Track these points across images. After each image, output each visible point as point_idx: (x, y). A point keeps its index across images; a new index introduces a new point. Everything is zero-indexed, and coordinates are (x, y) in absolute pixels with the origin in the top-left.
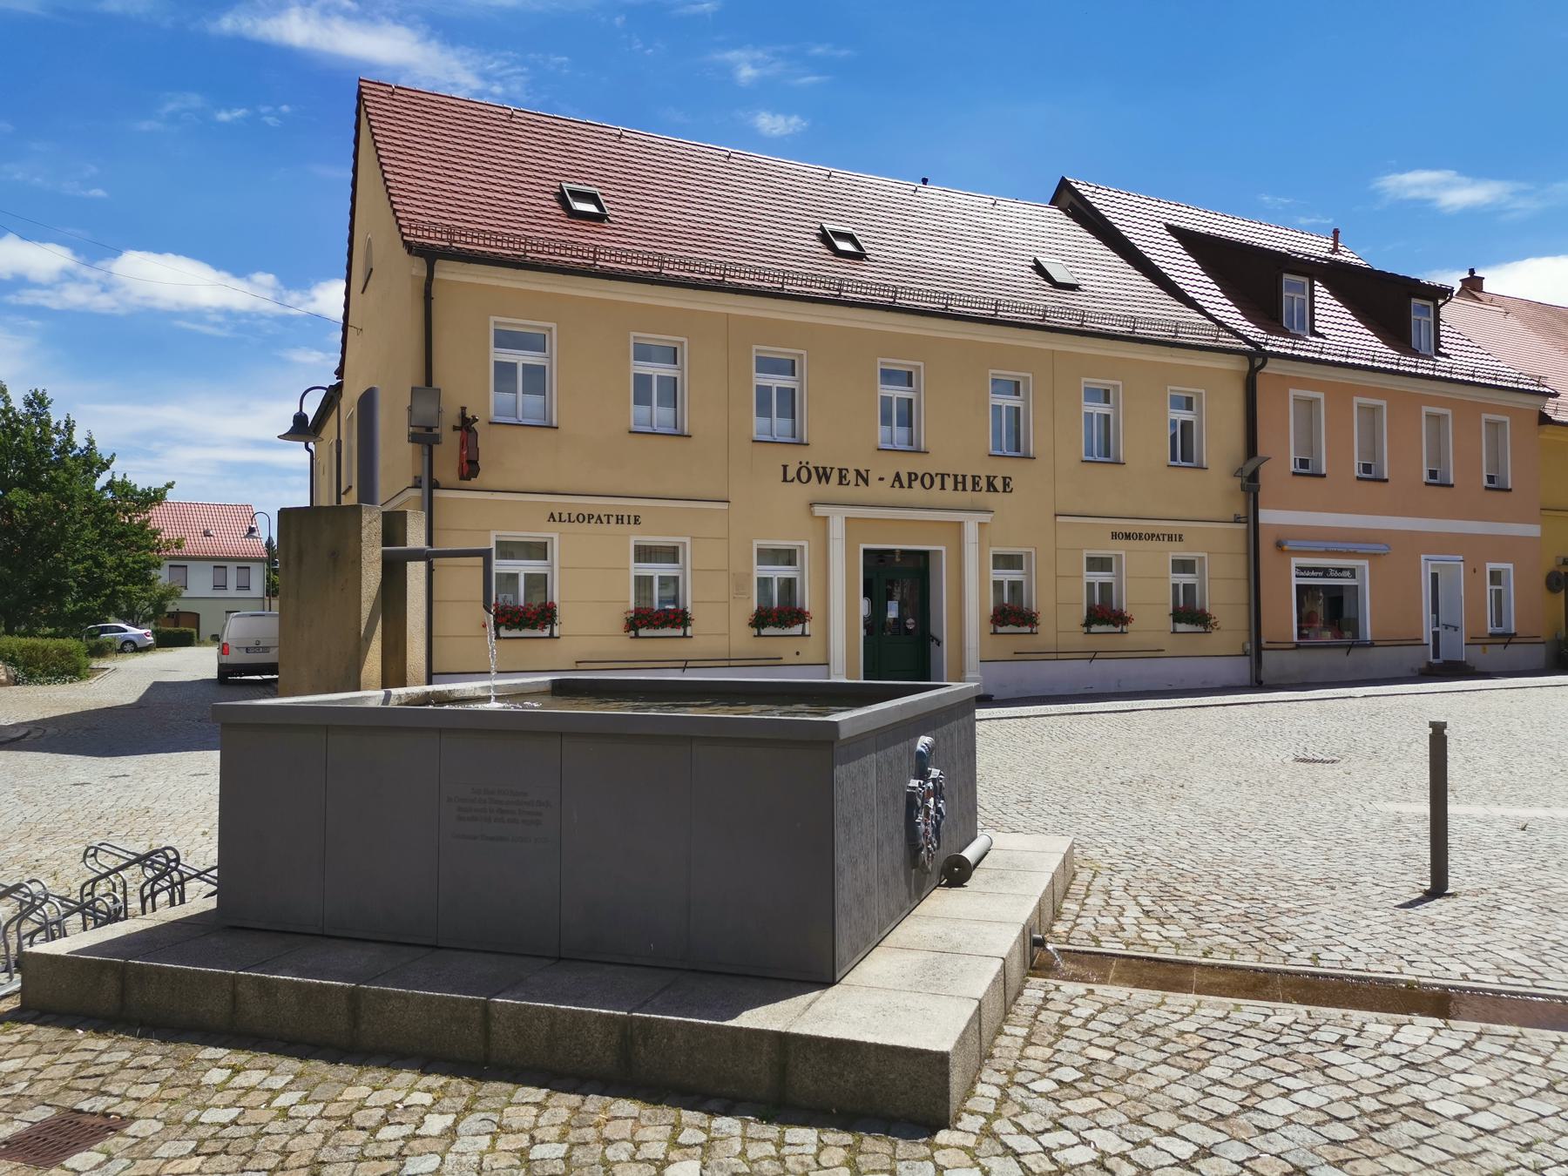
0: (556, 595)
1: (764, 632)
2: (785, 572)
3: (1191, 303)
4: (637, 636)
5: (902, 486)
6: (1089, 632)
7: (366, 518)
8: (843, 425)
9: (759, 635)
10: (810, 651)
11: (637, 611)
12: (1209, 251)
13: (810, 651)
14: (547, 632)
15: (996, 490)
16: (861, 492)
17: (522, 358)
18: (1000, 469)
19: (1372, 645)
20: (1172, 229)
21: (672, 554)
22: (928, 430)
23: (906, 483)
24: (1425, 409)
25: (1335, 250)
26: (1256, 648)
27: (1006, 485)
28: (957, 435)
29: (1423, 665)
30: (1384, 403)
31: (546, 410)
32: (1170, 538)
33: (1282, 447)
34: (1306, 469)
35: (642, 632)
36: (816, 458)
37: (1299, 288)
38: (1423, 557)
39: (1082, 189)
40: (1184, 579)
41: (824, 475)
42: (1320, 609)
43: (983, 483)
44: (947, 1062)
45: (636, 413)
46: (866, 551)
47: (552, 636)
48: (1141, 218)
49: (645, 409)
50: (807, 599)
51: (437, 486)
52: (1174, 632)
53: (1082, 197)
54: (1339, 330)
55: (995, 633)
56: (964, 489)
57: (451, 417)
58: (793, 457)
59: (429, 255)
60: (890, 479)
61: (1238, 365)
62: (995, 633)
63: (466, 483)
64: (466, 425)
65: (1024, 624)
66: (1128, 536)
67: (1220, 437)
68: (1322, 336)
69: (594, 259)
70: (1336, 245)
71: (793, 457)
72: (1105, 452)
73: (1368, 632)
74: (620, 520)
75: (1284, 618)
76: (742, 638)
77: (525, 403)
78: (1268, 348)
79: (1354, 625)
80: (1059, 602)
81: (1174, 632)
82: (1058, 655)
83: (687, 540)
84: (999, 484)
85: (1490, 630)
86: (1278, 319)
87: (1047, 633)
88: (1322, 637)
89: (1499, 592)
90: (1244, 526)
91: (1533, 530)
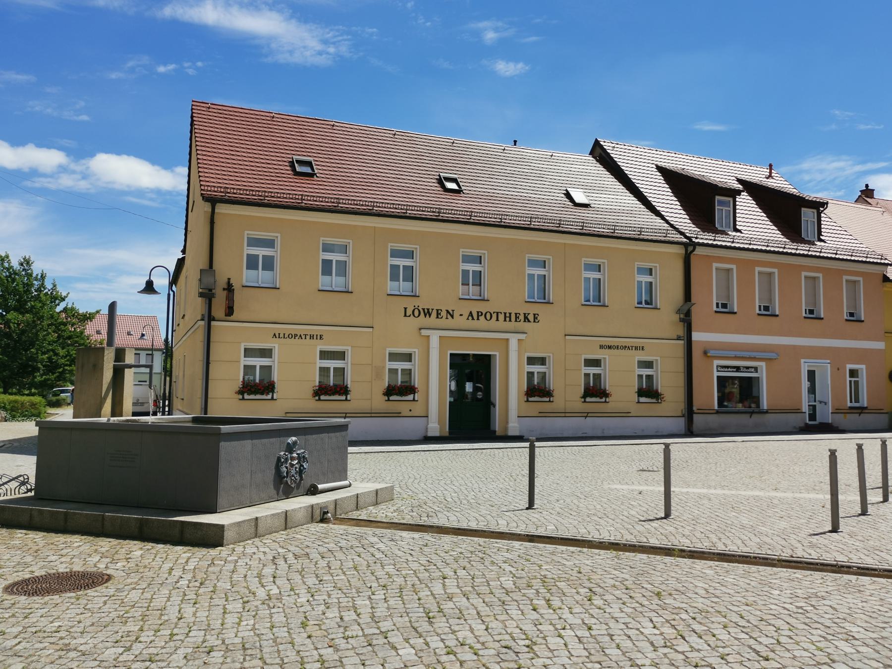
0: (275, 377)
1: (391, 398)
2: (406, 365)
3: (658, 213)
4: (319, 400)
5: (473, 319)
6: (585, 402)
7: (106, 352)
8: (439, 285)
9: (389, 400)
10: (418, 409)
11: (320, 386)
12: (675, 180)
13: (418, 409)
14: (269, 397)
15: (529, 321)
16: (450, 322)
17: (261, 252)
18: (531, 310)
19: (767, 412)
20: (660, 169)
21: (341, 355)
22: (488, 289)
23: (475, 317)
24: (804, 274)
25: (770, 176)
26: (689, 413)
27: (535, 318)
28: (506, 290)
29: (802, 425)
30: (776, 271)
31: (274, 281)
32: (636, 348)
33: (708, 296)
34: (724, 308)
35: (322, 397)
36: (423, 304)
37: (726, 204)
38: (802, 361)
39: (607, 146)
40: (646, 372)
41: (428, 313)
42: (735, 389)
43: (522, 317)
44: (223, 531)
45: (324, 281)
46: (451, 355)
47: (272, 399)
48: (641, 161)
49: (328, 278)
50: (417, 382)
51: (214, 320)
52: (639, 402)
53: (605, 149)
54: (753, 225)
55: (528, 401)
56: (510, 320)
57: (222, 283)
58: (410, 304)
59: (212, 201)
60: (466, 314)
61: (681, 250)
62: (528, 401)
63: (228, 318)
64: (229, 288)
65: (406, 394)
66: (610, 347)
67: (669, 292)
68: (739, 231)
69: (302, 199)
70: (771, 173)
71: (410, 304)
72: (596, 298)
73: (765, 405)
74: (312, 337)
75: (708, 394)
76: (379, 402)
77: (262, 276)
78: (697, 241)
79: (757, 400)
80: (567, 387)
81: (639, 402)
82: (565, 414)
83: (349, 348)
84: (531, 317)
85: (849, 404)
86: (713, 222)
87: (559, 401)
88: (738, 405)
89: (856, 383)
90: (682, 342)
91: (880, 345)
